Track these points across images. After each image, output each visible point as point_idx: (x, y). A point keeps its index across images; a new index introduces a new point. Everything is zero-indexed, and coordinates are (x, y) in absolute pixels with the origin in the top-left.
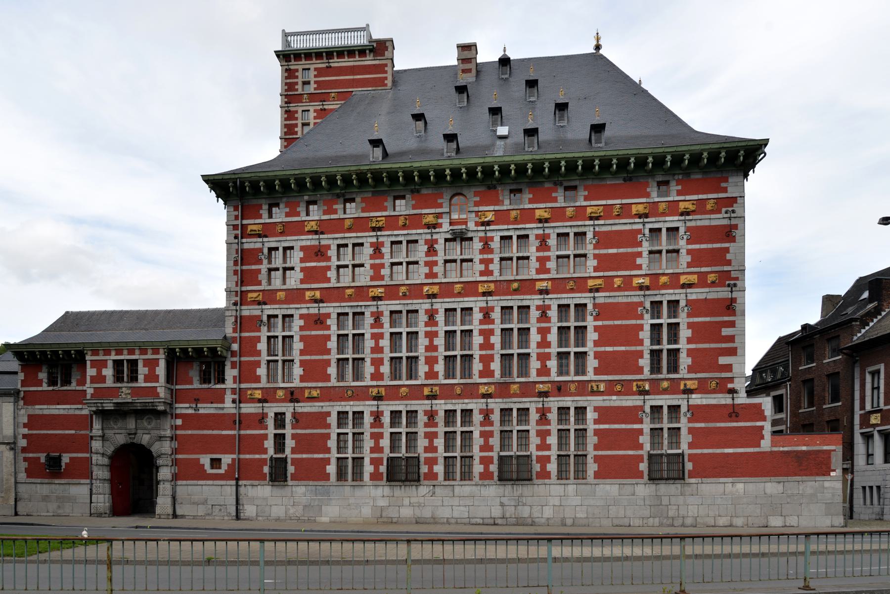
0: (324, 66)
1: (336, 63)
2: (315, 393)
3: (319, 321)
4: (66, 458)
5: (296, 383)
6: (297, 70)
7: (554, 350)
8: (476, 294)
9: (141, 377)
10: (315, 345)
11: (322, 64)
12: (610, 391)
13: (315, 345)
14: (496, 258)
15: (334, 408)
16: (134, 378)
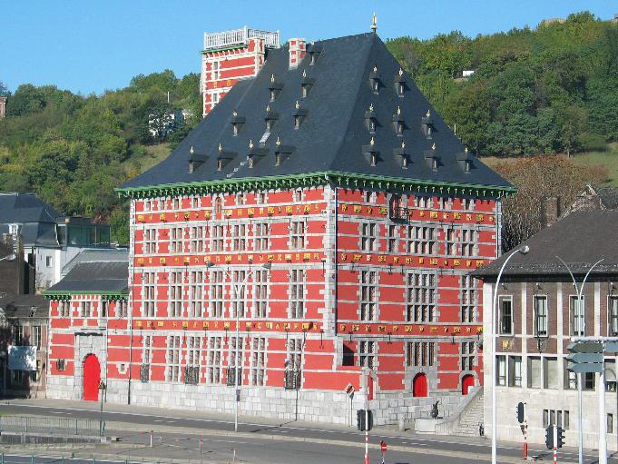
0: (223, 59)
1: (231, 57)
2: (161, 324)
3: (164, 277)
4: (66, 361)
5: (155, 318)
6: (211, 64)
7: (254, 300)
8: (223, 262)
9: (91, 313)
10: (163, 292)
11: (220, 59)
12: (274, 329)
13: (163, 292)
14: (232, 238)
15: (169, 333)
16: (89, 315)
